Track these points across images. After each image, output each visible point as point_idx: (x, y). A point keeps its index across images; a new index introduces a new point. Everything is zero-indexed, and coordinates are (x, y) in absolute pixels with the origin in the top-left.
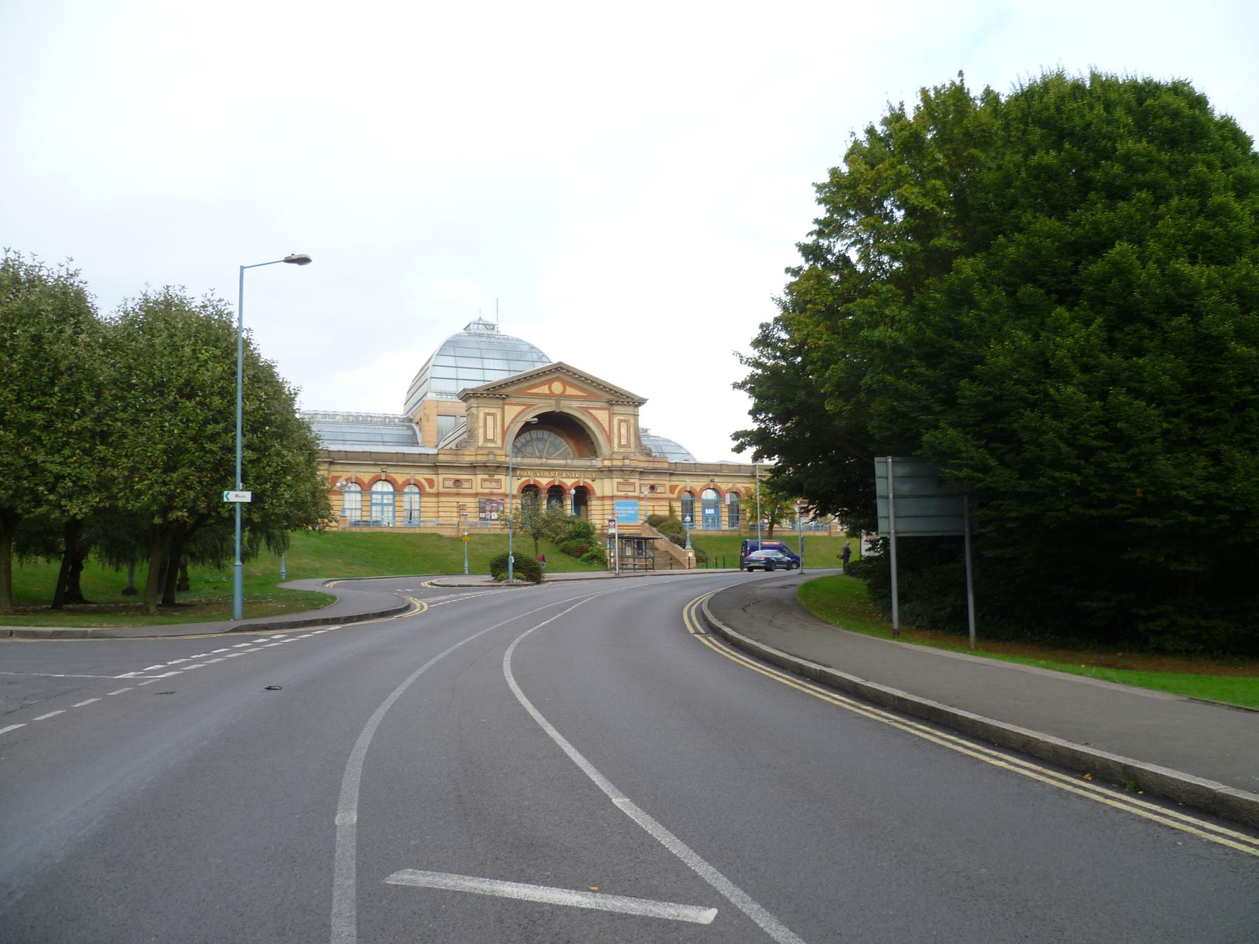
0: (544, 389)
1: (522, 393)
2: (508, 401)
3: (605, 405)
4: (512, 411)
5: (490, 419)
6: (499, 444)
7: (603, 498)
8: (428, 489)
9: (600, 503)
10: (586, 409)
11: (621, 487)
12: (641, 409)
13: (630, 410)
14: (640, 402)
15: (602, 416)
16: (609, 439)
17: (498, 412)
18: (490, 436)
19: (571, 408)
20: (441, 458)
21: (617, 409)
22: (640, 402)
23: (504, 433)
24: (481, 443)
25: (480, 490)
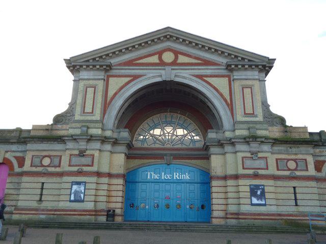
0: (155, 59)
1: (130, 63)
2: (114, 72)
3: (225, 72)
4: (115, 84)
5: (90, 90)
6: (97, 116)
7: (225, 178)
8: (17, 169)
9: (221, 183)
10: (200, 77)
11: (248, 163)
12: (271, 79)
13: (255, 74)
14: (265, 66)
15: (222, 84)
16: (231, 106)
17: (101, 85)
18: (88, 109)
19: (185, 77)
20: (32, 134)
21: (236, 75)
22: (265, 66)
23: (106, 105)
24: (77, 117)
25: (68, 169)
